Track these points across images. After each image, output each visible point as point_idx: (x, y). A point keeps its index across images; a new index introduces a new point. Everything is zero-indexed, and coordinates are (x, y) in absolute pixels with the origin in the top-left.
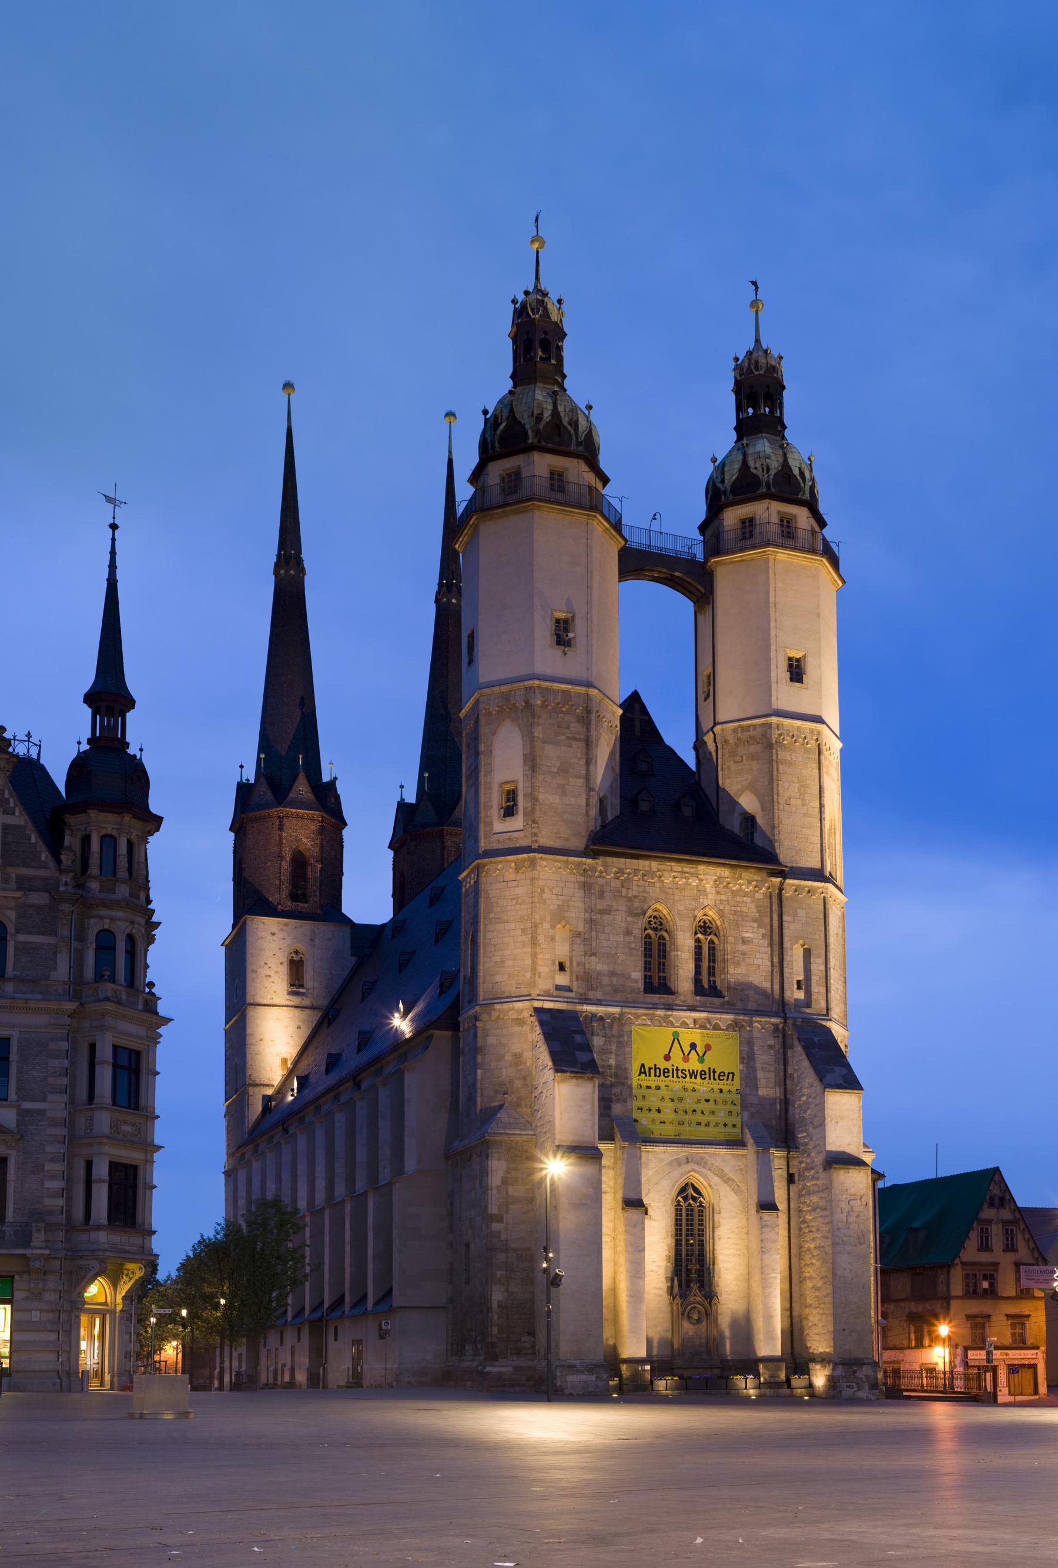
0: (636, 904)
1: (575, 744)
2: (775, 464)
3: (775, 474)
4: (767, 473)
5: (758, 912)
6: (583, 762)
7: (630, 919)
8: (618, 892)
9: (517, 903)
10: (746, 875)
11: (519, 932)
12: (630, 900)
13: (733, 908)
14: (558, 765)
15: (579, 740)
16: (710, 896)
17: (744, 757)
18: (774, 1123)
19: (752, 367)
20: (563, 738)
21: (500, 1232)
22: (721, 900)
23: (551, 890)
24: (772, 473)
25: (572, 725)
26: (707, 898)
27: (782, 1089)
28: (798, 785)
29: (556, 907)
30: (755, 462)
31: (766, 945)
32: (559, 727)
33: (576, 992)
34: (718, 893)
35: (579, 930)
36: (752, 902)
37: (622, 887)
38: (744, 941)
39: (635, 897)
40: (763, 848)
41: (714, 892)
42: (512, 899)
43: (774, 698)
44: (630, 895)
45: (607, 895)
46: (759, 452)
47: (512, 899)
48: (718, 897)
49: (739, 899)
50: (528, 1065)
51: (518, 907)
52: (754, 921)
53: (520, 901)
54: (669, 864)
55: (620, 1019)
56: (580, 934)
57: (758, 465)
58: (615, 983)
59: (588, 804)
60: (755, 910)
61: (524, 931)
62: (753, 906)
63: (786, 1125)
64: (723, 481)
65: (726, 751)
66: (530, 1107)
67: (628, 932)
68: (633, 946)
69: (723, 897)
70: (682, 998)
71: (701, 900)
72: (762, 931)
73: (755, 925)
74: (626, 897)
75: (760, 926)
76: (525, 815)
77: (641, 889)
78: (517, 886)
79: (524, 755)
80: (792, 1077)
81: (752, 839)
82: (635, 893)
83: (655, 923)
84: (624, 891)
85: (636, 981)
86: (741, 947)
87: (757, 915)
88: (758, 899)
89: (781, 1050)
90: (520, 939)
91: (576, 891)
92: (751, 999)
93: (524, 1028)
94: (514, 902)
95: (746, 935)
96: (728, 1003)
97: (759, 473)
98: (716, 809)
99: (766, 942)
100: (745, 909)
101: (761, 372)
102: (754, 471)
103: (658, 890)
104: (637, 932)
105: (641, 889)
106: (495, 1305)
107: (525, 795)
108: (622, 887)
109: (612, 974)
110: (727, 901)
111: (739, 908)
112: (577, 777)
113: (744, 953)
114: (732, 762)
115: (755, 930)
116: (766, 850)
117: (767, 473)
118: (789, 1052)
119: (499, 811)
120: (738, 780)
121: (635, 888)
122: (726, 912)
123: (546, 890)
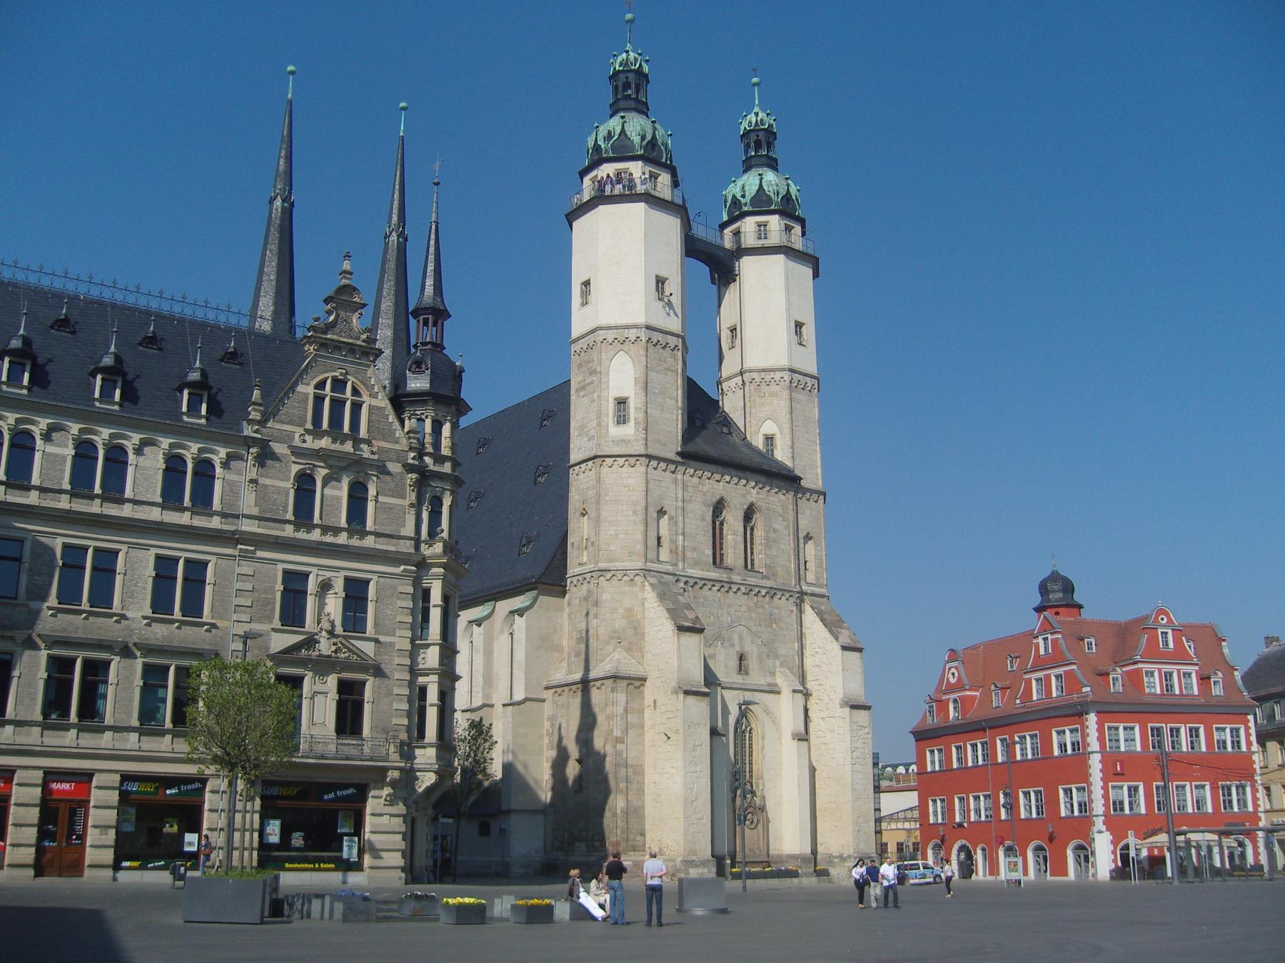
0: (708, 498)
1: (670, 373)
2: (783, 192)
4: (778, 195)
5: (783, 509)
6: (675, 387)
9: (629, 490)
11: (631, 513)
12: (704, 494)
14: (659, 387)
15: (672, 371)
17: (767, 394)
18: (795, 669)
19: (759, 122)
20: (662, 368)
21: (622, 751)
22: (760, 499)
23: (655, 483)
24: (780, 197)
27: (800, 644)
29: (657, 496)
30: (768, 187)
35: (672, 514)
39: (708, 492)
40: (781, 461)
42: (625, 487)
44: (704, 490)
45: (690, 489)
46: (770, 181)
47: (625, 487)
49: (771, 498)
50: (638, 617)
51: (629, 493)
53: (631, 489)
57: (771, 189)
58: (695, 556)
60: (780, 508)
61: (635, 513)
63: (803, 672)
64: (743, 196)
65: (752, 388)
66: (641, 651)
68: (706, 529)
69: (761, 497)
73: (781, 519)
74: (701, 491)
76: (635, 423)
78: (629, 477)
79: (635, 378)
80: (805, 634)
81: (772, 455)
84: (700, 486)
89: (799, 614)
90: (632, 518)
91: (670, 484)
93: (635, 588)
94: (627, 489)
95: (776, 526)
97: (772, 195)
98: (744, 431)
100: (774, 507)
101: (766, 127)
102: (768, 193)
103: (722, 488)
105: (711, 486)
106: (619, 811)
107: (636, 409)
108: (700, 483)
109: (694, 549)
110: (763, 499)
112: (670, 398)
114: (757, 397)
116: (784, 463)
117: (778, 195)
118: (803, 615)
119: (613, 418)
120: (762, 409)
123: (651, 481)
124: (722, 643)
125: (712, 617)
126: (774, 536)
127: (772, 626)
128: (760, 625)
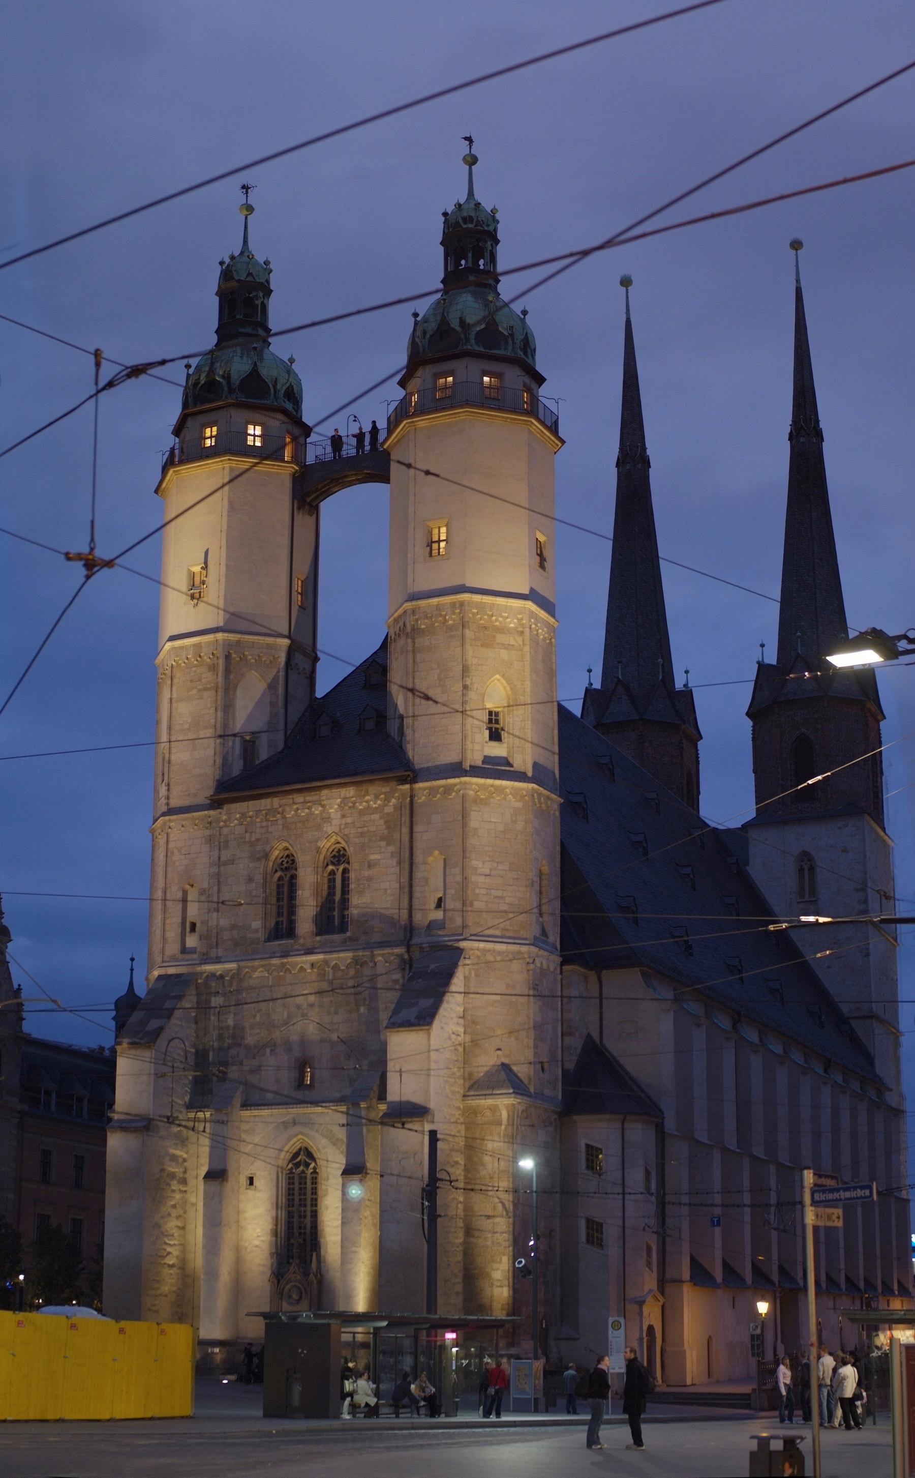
0: (259, 848)
3: (431, 336)
5: (388, 828)
7: (252, 865)
8: (242, 838)
10: (374, 789)
13: (360, 830)
16: (334, 822)
23: (179, 851)
24: (428, 336)
25: (204, 676)
26: (331, 825)
28: (438, 671)
31: (395, 864)
32: (191, 681)
33: (199, 952)
34: (343, 816)
36: (381, 818)
37: (246, 832)
38: (370, 866)
39: (258, 840)
41: (339, 816)
43: (410, 581)
48: (344, 821)
49: (365, 818)
52: (382, 838)
54: (291, 796)
55: (238, 975)
56: (204, 891)
59: (215, 754)
60: (384, 827)
62: (382, 822)
67: (250, 880)
68: (254, 893)
69: (349, 820)
70: (302, 941)
71: (325, 829)
72: (391, 849)
73: (383, 843)
75: (388, 844)
77: (264, 830)
82: (258, 836)
83: (287, 862)
84: (248, 835)
85: (256, 931)
86: (366, 873)
87: (386, 832)
88: (388, 814)
92: (376, 930)
95: (373, 857)
96: (350, 938)
99: (394, 861)
100: (372, 829)
104: (259, 878)
105: (264, 830)
110: (353, 823)
111: (365, 829)
113: (370, 879)
115: (383, 850)
121: (258, 830)
122: (351, 836)
123: (176, 851)
124: (271, 1050)
125: (258, 1015)
126: (366, 873)
127: (358, 1010)
128: (336, 1013)
